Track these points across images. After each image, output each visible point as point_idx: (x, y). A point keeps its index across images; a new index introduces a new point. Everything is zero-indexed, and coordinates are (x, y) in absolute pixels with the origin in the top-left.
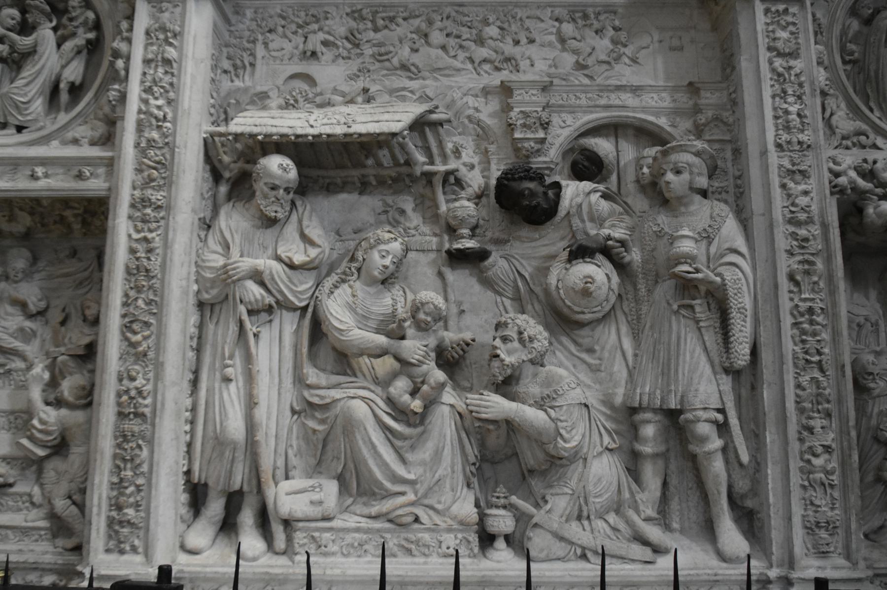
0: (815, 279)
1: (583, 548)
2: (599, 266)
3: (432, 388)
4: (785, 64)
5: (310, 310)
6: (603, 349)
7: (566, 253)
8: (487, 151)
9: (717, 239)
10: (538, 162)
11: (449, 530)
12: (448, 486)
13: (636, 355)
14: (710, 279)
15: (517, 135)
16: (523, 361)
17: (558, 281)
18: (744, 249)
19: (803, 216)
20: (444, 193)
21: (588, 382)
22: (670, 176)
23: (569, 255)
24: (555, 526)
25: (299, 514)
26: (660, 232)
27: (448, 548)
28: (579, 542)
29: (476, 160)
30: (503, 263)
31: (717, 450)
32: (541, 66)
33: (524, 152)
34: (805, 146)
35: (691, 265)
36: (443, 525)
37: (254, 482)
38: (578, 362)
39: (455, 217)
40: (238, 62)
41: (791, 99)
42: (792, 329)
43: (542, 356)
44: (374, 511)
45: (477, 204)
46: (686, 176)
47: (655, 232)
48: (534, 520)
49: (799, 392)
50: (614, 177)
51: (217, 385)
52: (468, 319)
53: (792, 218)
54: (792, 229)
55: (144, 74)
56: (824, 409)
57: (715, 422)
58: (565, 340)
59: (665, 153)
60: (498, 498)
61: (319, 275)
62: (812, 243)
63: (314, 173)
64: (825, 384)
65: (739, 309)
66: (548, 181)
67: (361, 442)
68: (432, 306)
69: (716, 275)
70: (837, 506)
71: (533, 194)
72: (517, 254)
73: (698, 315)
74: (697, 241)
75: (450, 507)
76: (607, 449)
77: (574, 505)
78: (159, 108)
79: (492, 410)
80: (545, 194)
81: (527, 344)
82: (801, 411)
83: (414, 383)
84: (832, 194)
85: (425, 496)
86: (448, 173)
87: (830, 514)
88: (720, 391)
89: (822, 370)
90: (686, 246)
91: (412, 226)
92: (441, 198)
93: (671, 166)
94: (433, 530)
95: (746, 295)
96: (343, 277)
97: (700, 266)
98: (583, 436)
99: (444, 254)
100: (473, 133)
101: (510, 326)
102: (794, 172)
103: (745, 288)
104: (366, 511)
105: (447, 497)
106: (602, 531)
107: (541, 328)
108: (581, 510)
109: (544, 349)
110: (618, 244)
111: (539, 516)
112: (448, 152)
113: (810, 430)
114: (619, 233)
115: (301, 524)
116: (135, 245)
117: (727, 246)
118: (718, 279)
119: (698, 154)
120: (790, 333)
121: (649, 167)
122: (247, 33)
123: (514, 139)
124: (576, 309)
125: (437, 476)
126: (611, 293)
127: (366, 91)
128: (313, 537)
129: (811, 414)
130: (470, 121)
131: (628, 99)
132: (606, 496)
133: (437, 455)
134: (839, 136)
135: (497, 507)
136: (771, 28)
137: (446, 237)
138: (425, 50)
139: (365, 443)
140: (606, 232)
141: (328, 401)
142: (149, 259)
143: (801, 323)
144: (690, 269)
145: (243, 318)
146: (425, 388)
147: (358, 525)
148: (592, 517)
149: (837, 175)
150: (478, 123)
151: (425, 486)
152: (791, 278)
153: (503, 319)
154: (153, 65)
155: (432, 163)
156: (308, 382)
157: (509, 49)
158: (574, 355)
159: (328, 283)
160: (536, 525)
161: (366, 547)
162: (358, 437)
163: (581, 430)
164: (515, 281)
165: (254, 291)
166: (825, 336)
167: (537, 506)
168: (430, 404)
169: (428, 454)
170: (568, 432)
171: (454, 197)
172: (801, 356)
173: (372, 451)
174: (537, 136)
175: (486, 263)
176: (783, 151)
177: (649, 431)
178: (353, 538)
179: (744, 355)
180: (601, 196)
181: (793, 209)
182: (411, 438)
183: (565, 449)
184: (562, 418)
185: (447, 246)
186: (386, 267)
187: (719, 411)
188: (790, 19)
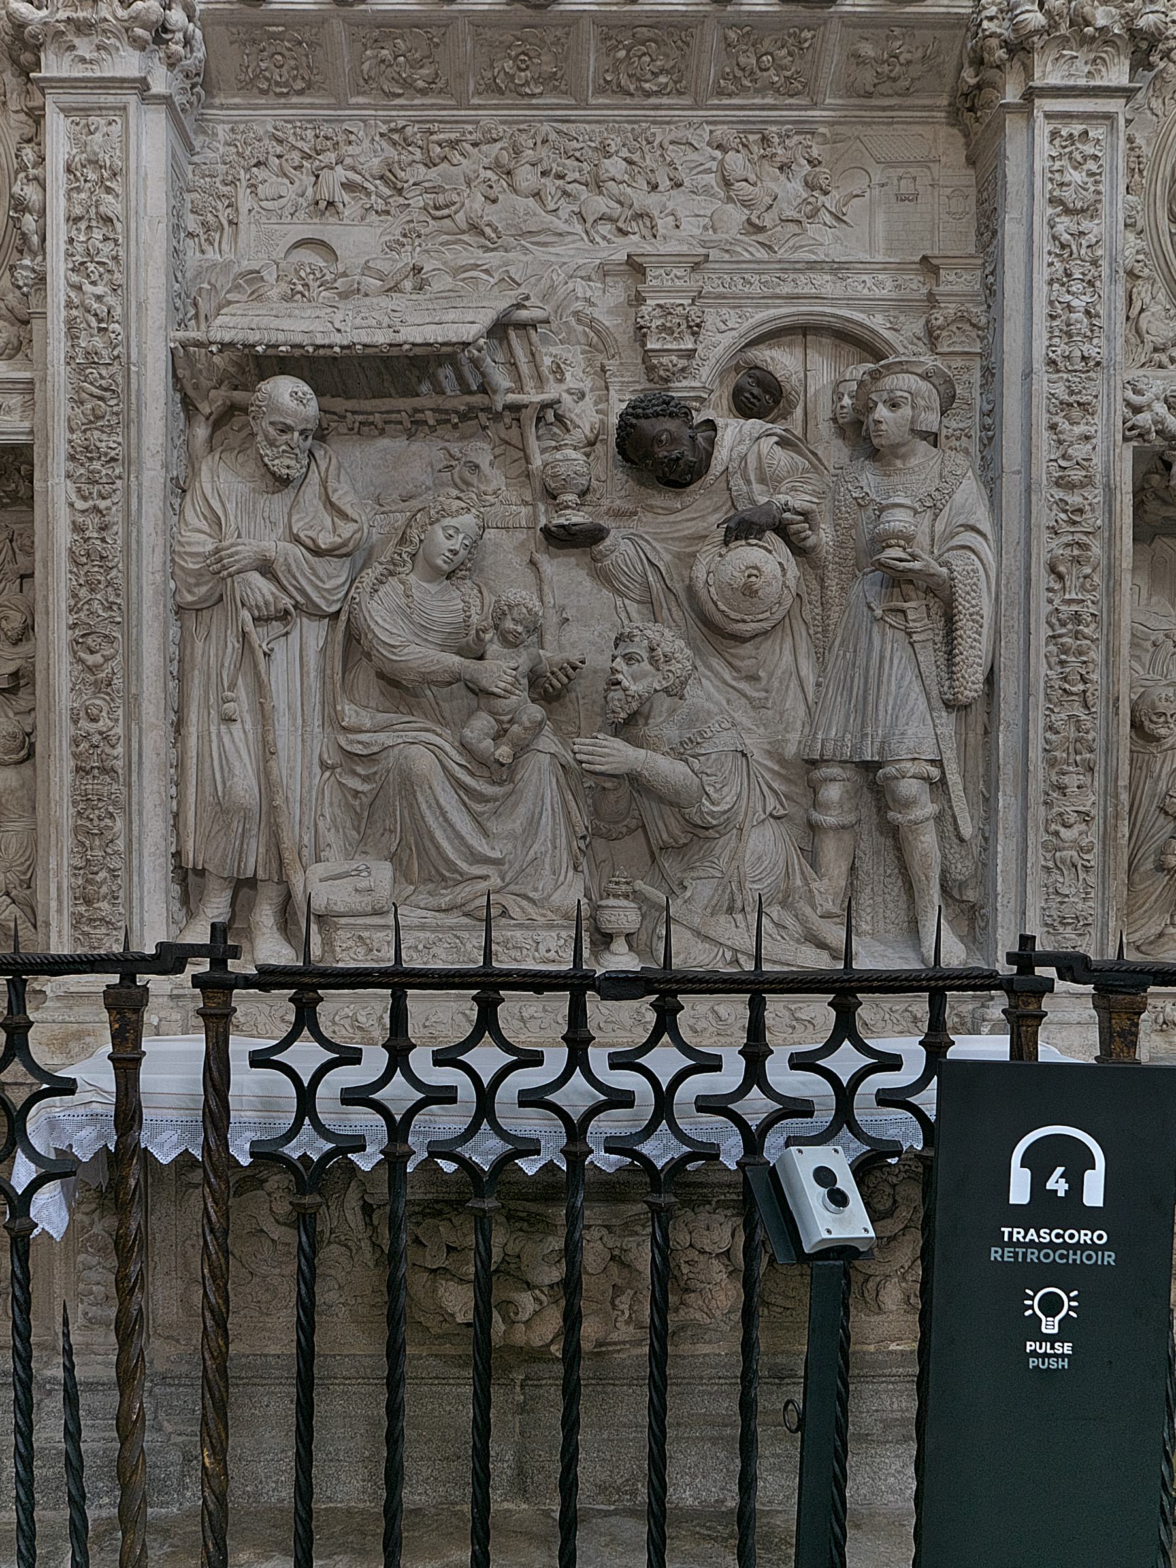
0: (1088, 570)
2: (770, 552)
3: (525, 729)
4: (1074, 228)
5: (343, 617)
6: (771, 675)
7: (722, 531)
8: (603, 369)
11: (550, 926)
12: (547, 867)
17: (708, 573)
18: (986, 526)
19: (1077, 475)
21: (747, 723)
22: (882, 412)
25: (341, 908)
27: (548, 951)
30: (626, 547)
31: (927, 819)
32: (691, 227)
34: (1092, 363)
36: (541, 920)
38: (734, 695)
39: (555, 476)
40: (210, 217)
41: (1076, 287)
42: (1047, 645)
43: (683, 684)
44: (444, 902)
45: (588, 455)
46: (906, 411)
47: (855, 499)
49: (1048, 735)
50: (799, 412)
51: (213, 729)
52: (573, 632)
53: (1061, 477)
54: (1059, 494)
55: (71, 241)
56: (1083, 760)
57: (927, 779)
58: (715, 662)
59: (875, 376)
60: (617, 883)
61: (352, 567)
62: (1088, 515)
63: (340, 405)
64: (1089, 725)
65: (971, 615)
66: (698, 418)
67: (424, 806)
68: (524, 610)
70: (1092, 895)
71: (674, 440)
72: (647, 533)
73: (911, 624)
74: (916, 512)
77: (724, 891)
78: (99, 298)
79: (611, 759)
81: (661, 666)
82: (1052, 763)
84: (1126, 439)
85: (514, 881)
86: (545, 406)
87: (1080, 906)
88: (936, 734)
89: (1086, 706)
90: (899, 520)
91: (490, 490)
92: (533, 445)
93: (885, 396)
94: (527, 928)
95: (985, 594)
96: (391, 567)
97: (918, 551)
98: (739, 796)
101: (637, 639)
102: (1070, 405)
103: (983, 585)
104: (433, 902)
105: (546, 881)
110: (801, 518)
112: (545, 371)
113: (1062, 789)
114: (800, 501)
115: (343, 921)
116: (80, 519)
119: (926, 377)
120: (1043, 651)
121: (851, 397)
122: (222, 168)
123: (646, 351)
124: (733, 615)
127: (417, 270)
128: (360, 937)
129: (1065, 767)
130: (579, 321)
131: (825, 283)
133: (533, 824)
134: (1149, 347)
135: (616, 896)
136: (1057, 165)
137: (542, 507)
138: (507, 199)
139: (430, 807)
141: (376, 749)
142: (103, 540)
143: (1060, 636)
145: (247, 629)
149: (1137, 410)
150: (592, 323)
151: (517, 866)
152: (1053, 569)
154: (83, 225)
155: (521, 390)
157: (641, 198)
158: (725, 682)
161: (434, 950)
165: (262, 587)
166: (1096, 655)
168: (521, 749)
169: (518, 822)
170: (716, 791)
172: (1056, 685)
173: (441, 819)
176: (1058, 371)
177: (833, 793)
179: (974, 683)
181: (1063, 463)
183: (712, 814)
184: (709, 771)
185: (543, 521)
186: (455, 553)
187: (932, 762)
188: (1089, 149)
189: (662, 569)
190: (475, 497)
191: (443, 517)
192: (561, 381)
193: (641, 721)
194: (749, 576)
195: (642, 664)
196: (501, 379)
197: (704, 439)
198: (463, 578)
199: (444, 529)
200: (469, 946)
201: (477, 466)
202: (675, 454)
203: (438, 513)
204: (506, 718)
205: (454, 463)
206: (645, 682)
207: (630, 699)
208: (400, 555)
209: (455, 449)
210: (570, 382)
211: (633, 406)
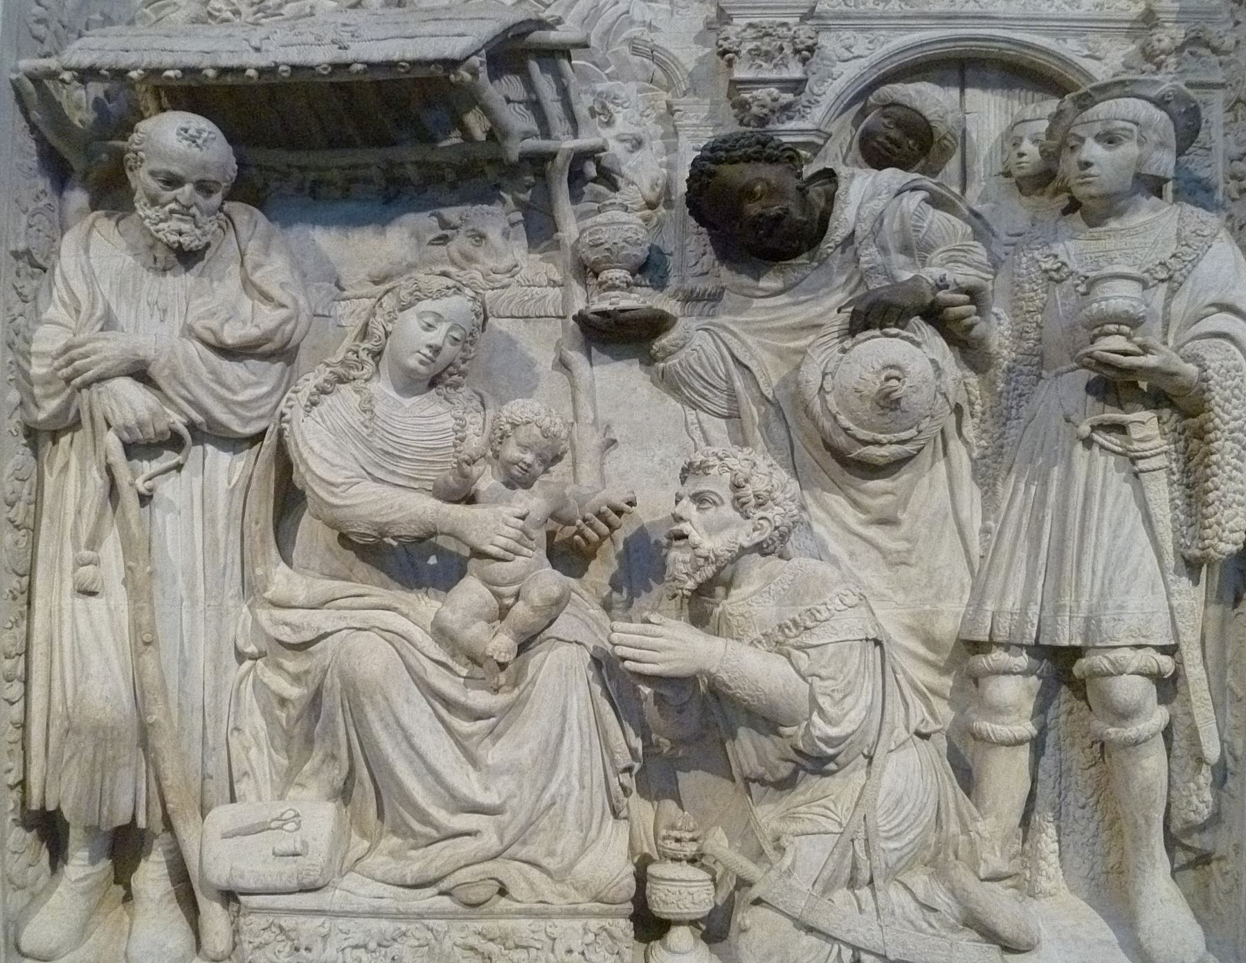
1: (856, 949)
2: (918, 345)
3: (534, 609)
9: (1189, 284)
10: (788, 131)
11: (574, 914)
13: (986, 531)
14: (1173, 368)
15: (740, 73)
16: (742, 548)
17: (824, 375)
20: (576, 197)
23: (852, 322)
24: (799, 906)
26: (1058, 270)
27: (570, 951)
28: (849, 938)
29: (652, 129)
30: (702, 341)
33: (755, 109)
35: (1129, 338)
36: (559, 904)
37: (158, 811)
38: (859, 547)
43: (783, 537)
45: (646, 220)
47: (1046, 271)
48: (755, 892)
58: (837, 502)
60: (678, 840)
65: (1232, 432)
67: (377, 727)
68: (537, 431)
69: (1186, 359)
72: (735, 322)
75: (572, 865)
76: (918, 734)
77: (843, 855)
79: (670, 655)
80: (802, 191)
83: (498, 596)
85: (522, 837)
86: (582, 156)
92: (564, 207)
98: (870, 709)
99: (572, 322)
100: (641, 75)
104: (397, 869)
105: (569, 842)
106: (898, 911)
107: (782, 475)
108: (855, 867)
109: (788, 521)
110: (966, 297)
111: (765, 883)
112: (582, 110)
114: (963, 275)
117: (1213, 297)
118: (1191, 369)
123: (734, 83)
124: (862, 434)
125: (547, 797)
126: (940, 399)
128: (281, 929)
130: (635, 51)
132: (911, 836)
137: (577, 289)
140: (932, 272)
141: (308, 636)
144: (1129, 347)
146: (520, 609)
147: (376, 903)
148: (878, 882)
150: (652, 53)
151: (522, 818)
153: (698, 458)
155: (546, 134)
156: (268, 595)
159: (309, 383)
160: (758, 902)
162: (372, 716)
163: (865, 700)
164: (729, 379)
167: (759, 856)
170: (836, 703)
171: (596, 206)
173: (404, 745)
174: (785, 75)
175: (664, 341)
178: (368, 933)
180: (925, 200)
182: (489, 717)
184: (823, 673)
185: (579, 305)
186: (436, 350)
189: (754, 369)
190: (479, 277)
191: (419, 300)
192: (609, 123)
193: (720, 591)
194: (888, 379)
195: (722, 509)
196: (518, 120)
197: (819, 195)
198: (456, 386)
199: (420, 316)
200: (447, 943)
201: (483, 236)
202: (774, 210)
203: (411, 294)
204: (512, 589)
205: (448, 232)
206: (727, 535)
207: (701, 561)
208: (356, 352)
209: (452, 214)
210: (623, 123)
211: (713, 148)
